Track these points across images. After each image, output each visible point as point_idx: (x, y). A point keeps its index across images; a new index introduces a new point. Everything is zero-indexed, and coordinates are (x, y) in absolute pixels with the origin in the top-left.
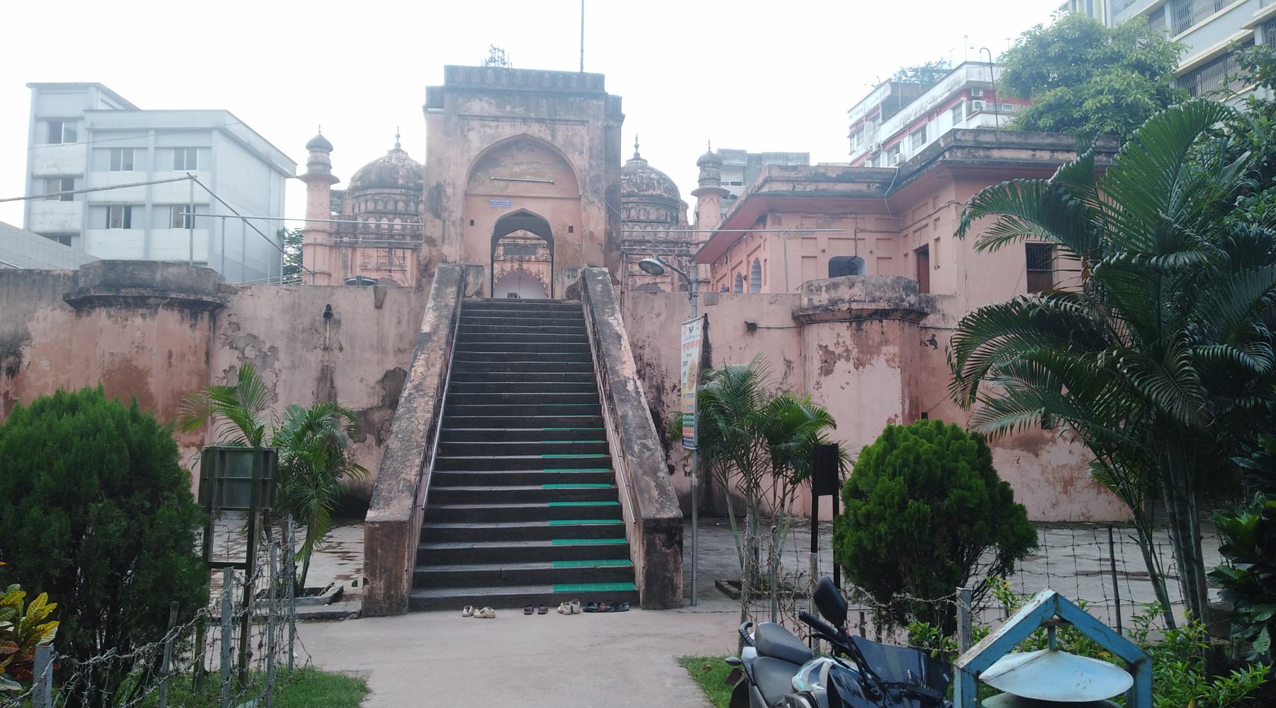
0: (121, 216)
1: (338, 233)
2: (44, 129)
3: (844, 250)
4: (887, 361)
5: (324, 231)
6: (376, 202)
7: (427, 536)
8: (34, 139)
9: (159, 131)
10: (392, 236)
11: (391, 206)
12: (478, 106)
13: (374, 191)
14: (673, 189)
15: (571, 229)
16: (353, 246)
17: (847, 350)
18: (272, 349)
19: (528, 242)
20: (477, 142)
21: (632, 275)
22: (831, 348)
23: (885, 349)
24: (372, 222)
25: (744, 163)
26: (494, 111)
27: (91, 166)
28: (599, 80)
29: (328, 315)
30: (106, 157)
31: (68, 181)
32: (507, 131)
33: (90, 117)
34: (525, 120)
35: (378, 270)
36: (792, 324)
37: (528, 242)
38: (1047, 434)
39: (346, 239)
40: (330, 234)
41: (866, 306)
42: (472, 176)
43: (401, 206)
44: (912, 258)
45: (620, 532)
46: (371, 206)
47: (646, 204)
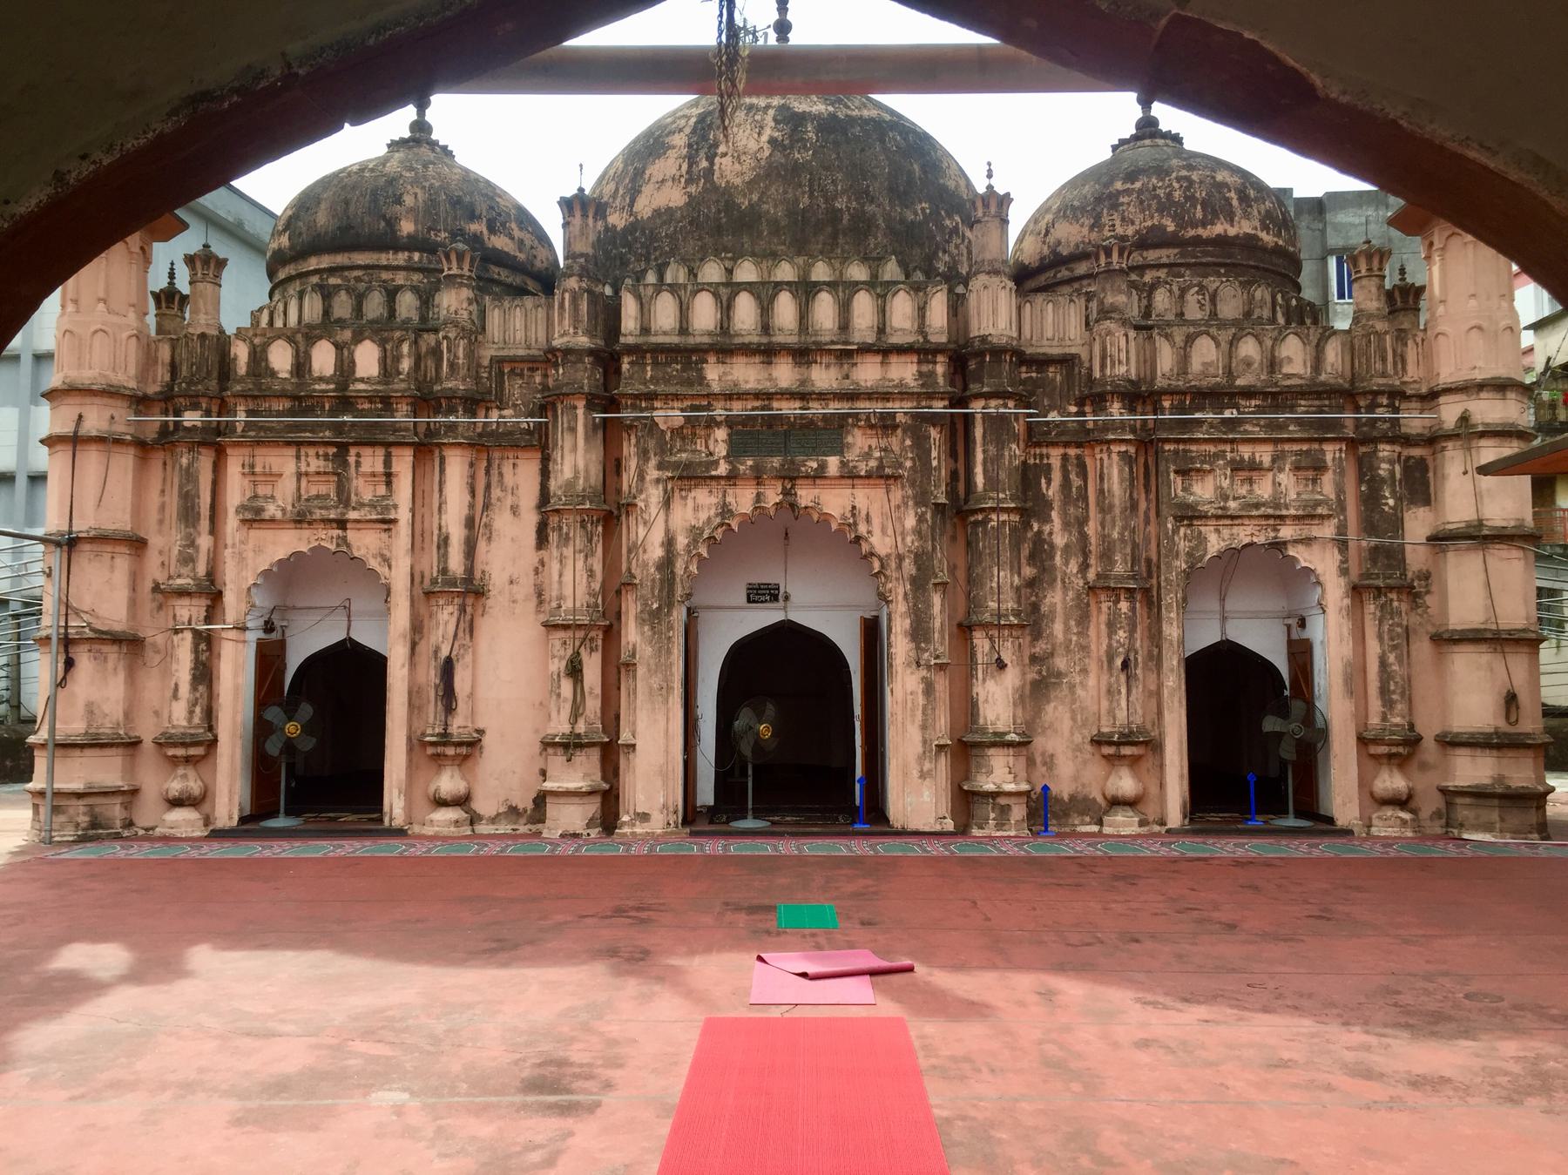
1: (168, 400)
5: (110, 392)
6: (327, 294)
10: (345, 402)
13: (325, 261)
16: (215, 441)
19: (816, 409)
21: (1189, 515)
24: (281, 358)
35: (300, 520)
37: (816, 409)
39: (191, 418)
40: (140, 402)
43: (407, 304)
46: (313, 308)
47: (1203, 269)
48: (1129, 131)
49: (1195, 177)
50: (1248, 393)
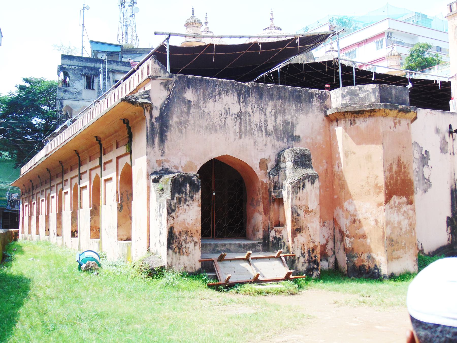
18: (426, 152)
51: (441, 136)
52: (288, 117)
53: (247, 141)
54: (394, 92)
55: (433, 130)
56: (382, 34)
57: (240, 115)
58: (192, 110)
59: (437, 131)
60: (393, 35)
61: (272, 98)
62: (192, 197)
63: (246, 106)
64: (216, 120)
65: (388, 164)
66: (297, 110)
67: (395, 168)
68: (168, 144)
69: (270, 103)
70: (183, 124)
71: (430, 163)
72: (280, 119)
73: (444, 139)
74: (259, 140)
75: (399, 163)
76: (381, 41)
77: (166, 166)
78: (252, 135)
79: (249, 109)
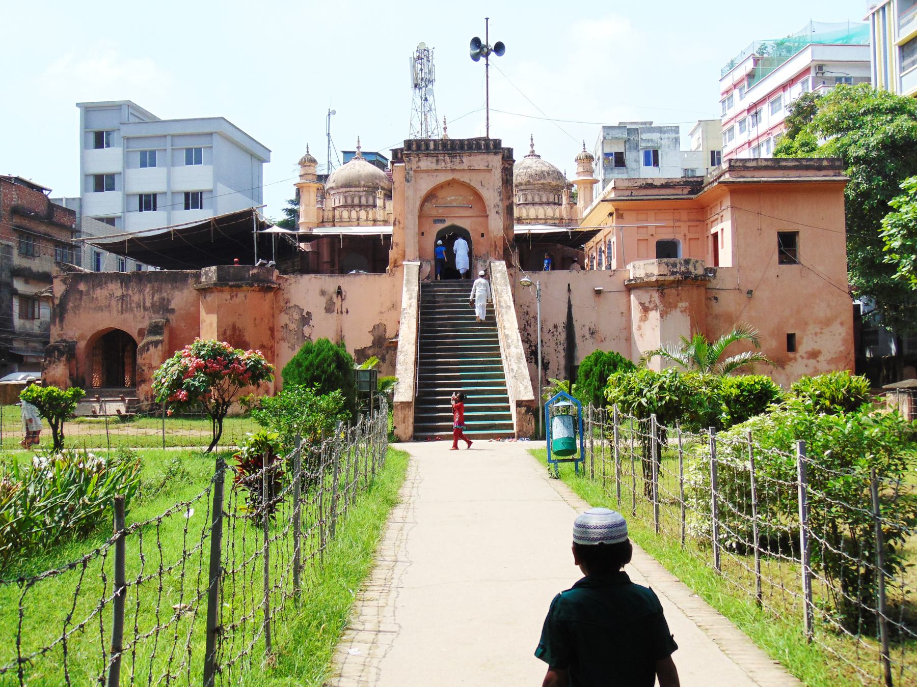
0: (148, 202)
2: (92, 139)
3: (666, 236)
4: (682, 312)
6: (346, 198)
7: (417, 410)
8: (85, 146)
9: (173, 136)
11: (356, 201)
12: (426, 163)
13: (344, 190)
14: (559, 176)
15: (482, 235)
17: (656, 306)
20: (426, 185)
22: (647, 305)
23: (680, 305)
25: (625, 136)
26: (434, 166)
27: (127, 164)
28: (497, 143)
29: (339, 292)
30: (138, 158)
31: (111, 177)
32: (443, 178)
33: (123, 128)
34: (453, 170)
36: (624, 289)
38: (791, 355)
41: (667, 278)
42: (422, 205)
44: (711, 239)
45: (508, 409)
47: (539, 190)
48: (528, 153)
49: (538, 169)
50: (541, 219)
51: (327, 297)
52: (165, 295)
53: (128, 316)
54: (232, 270)
55: (318, 292)
56: (807, 71)
57: (122, 297)
58: (84, 297)
59: (323, 293)
60: (824, 69)
61: (150, 282)
62: (59, 360)
63: (127, 290)
64: (103, 302)
65: (222, 330)
66: (173, 288)
67: (229, 332)
68: (66, 322)
69: (149, 285)
70: (77, 307)
71: (311, 323)
72: (156, 297)
73: (331, 299)
74: (138, 314)
75: (234, 328)
76: (807, 80)
77: (64, 337)
78: (132, 310)
79: (130, 292)
